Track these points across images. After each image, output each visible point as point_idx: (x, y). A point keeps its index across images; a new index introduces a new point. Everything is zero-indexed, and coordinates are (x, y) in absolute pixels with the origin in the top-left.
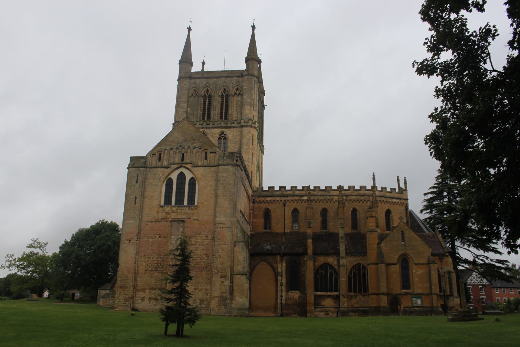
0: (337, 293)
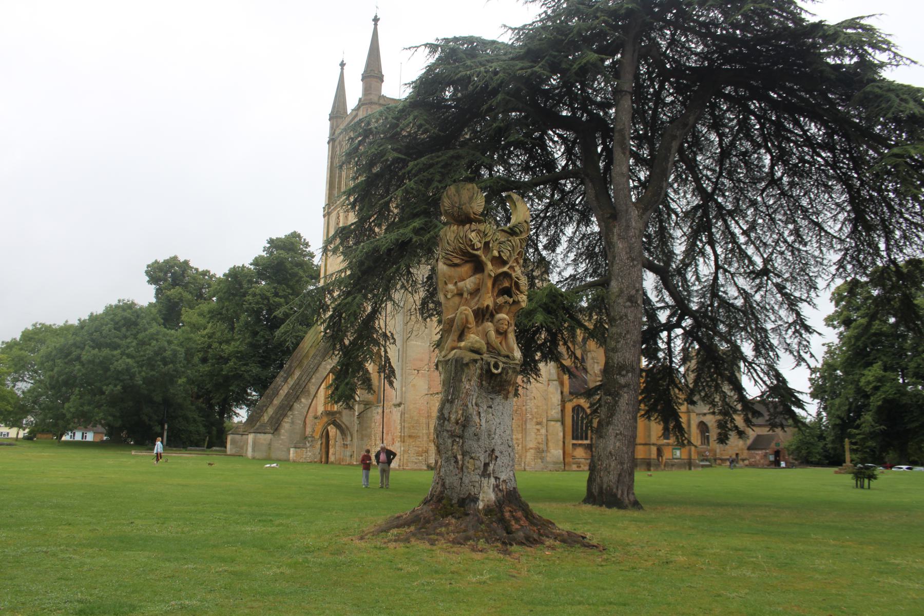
0: (588, 442)
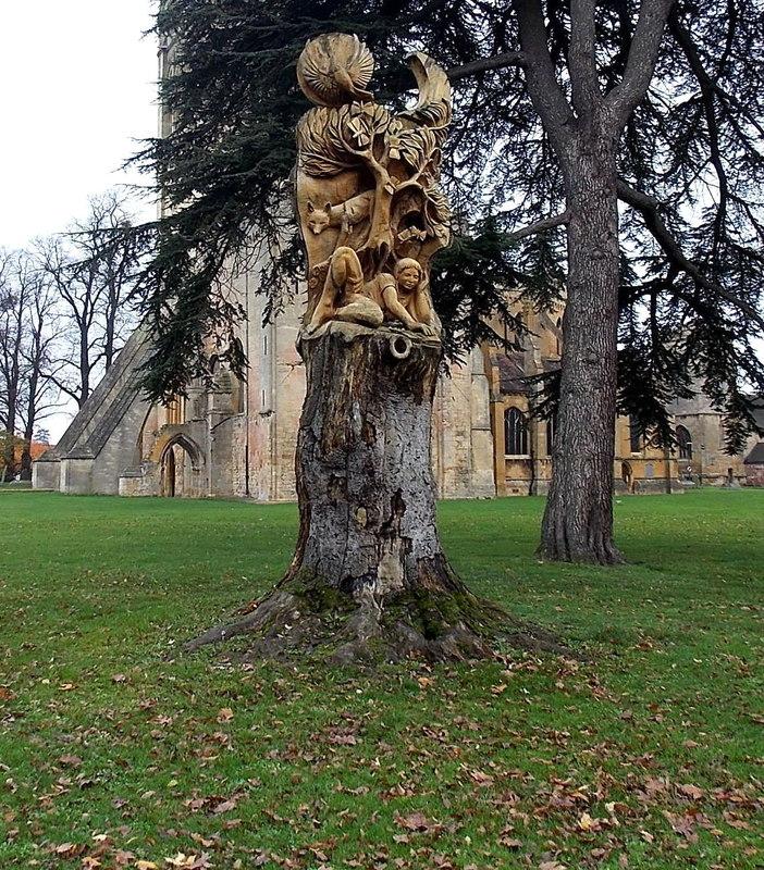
0: (527, 457)
